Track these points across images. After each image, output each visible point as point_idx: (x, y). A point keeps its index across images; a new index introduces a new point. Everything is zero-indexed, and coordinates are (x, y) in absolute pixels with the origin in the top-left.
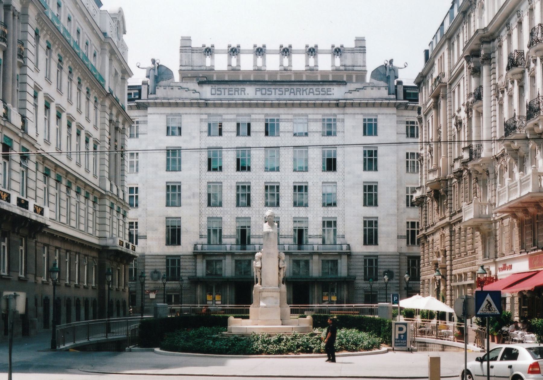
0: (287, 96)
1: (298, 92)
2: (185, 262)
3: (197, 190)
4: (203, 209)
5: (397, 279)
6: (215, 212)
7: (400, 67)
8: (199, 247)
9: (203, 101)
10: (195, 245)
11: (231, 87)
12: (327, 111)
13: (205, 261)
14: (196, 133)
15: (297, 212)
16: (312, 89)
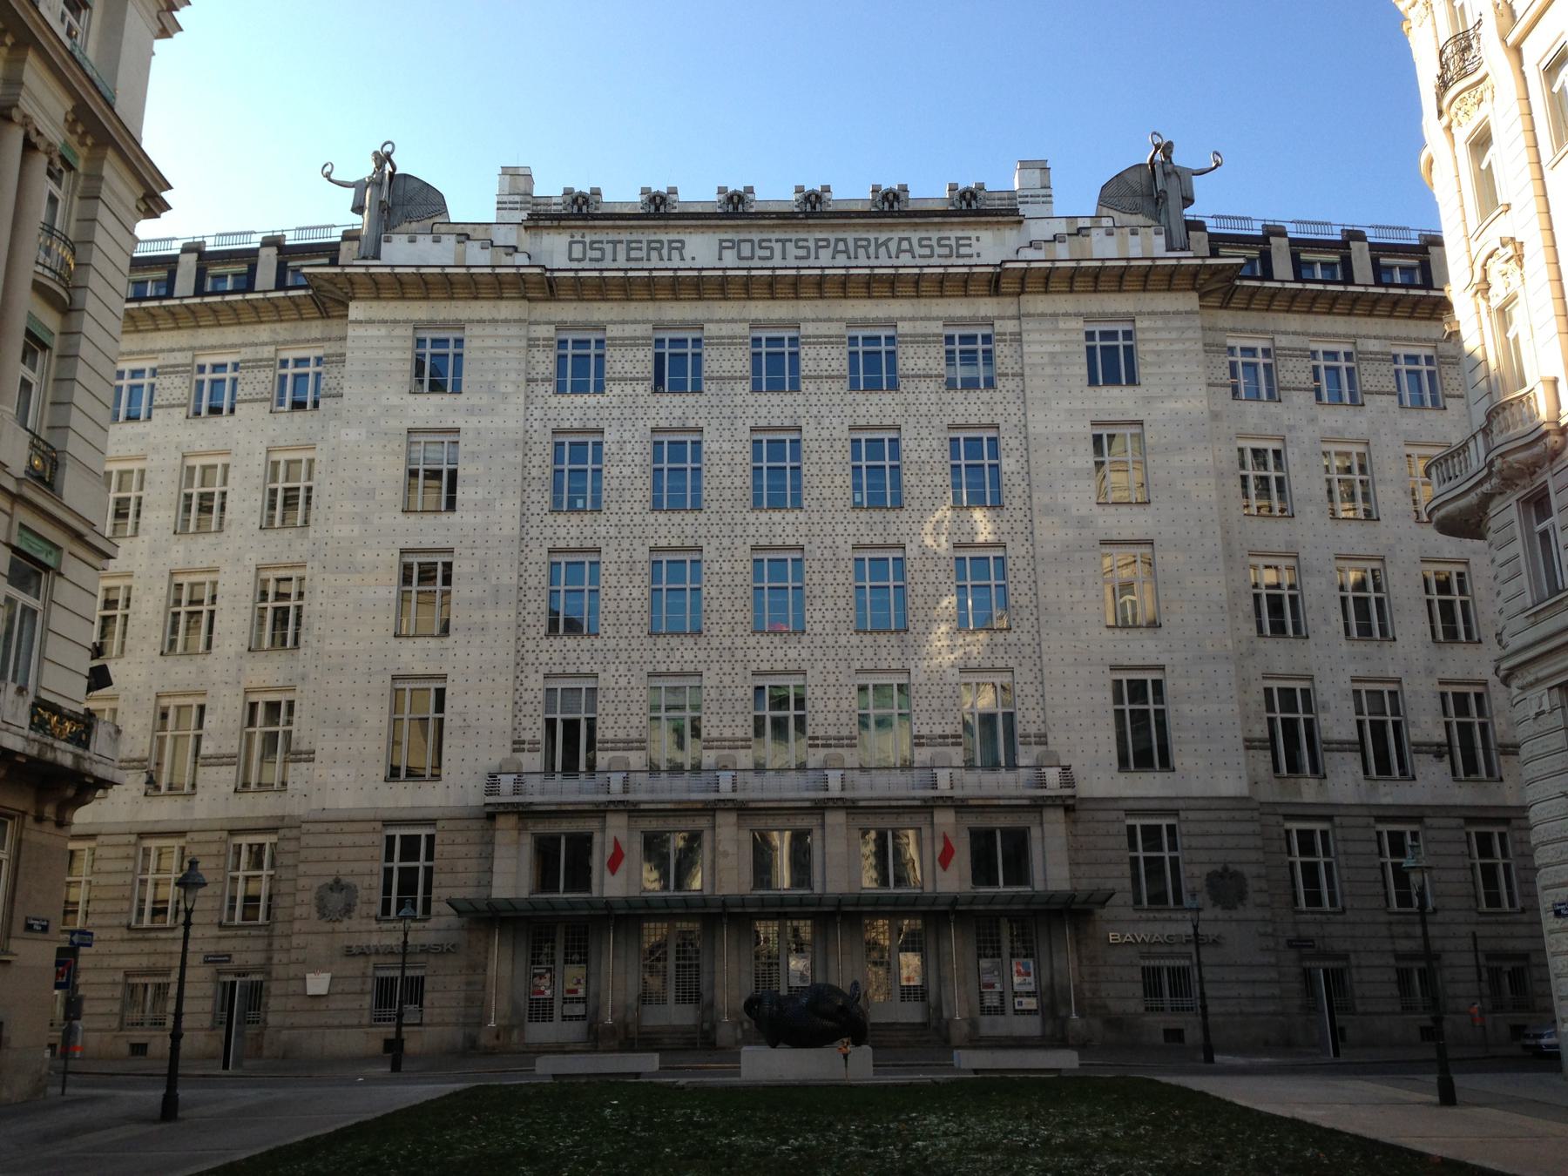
0: (825, 258)
1: (861, 252)
2: (453, 843)
3: (509, 578)
4: (530, 645)
5: (1262, 906)
6: (570, 652)
7: (1196, 167)
8: (507, 782)
9: (538, 270)
10: (492, 776)
11: (634, 237)
12: (959, 308)
13: (527, 842)
14: (511, 383)
15: (869, 653)
16: (908, 239)
